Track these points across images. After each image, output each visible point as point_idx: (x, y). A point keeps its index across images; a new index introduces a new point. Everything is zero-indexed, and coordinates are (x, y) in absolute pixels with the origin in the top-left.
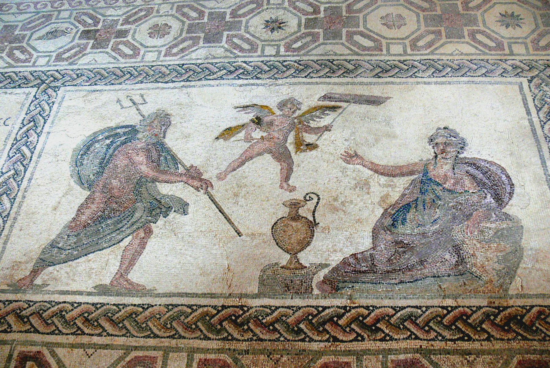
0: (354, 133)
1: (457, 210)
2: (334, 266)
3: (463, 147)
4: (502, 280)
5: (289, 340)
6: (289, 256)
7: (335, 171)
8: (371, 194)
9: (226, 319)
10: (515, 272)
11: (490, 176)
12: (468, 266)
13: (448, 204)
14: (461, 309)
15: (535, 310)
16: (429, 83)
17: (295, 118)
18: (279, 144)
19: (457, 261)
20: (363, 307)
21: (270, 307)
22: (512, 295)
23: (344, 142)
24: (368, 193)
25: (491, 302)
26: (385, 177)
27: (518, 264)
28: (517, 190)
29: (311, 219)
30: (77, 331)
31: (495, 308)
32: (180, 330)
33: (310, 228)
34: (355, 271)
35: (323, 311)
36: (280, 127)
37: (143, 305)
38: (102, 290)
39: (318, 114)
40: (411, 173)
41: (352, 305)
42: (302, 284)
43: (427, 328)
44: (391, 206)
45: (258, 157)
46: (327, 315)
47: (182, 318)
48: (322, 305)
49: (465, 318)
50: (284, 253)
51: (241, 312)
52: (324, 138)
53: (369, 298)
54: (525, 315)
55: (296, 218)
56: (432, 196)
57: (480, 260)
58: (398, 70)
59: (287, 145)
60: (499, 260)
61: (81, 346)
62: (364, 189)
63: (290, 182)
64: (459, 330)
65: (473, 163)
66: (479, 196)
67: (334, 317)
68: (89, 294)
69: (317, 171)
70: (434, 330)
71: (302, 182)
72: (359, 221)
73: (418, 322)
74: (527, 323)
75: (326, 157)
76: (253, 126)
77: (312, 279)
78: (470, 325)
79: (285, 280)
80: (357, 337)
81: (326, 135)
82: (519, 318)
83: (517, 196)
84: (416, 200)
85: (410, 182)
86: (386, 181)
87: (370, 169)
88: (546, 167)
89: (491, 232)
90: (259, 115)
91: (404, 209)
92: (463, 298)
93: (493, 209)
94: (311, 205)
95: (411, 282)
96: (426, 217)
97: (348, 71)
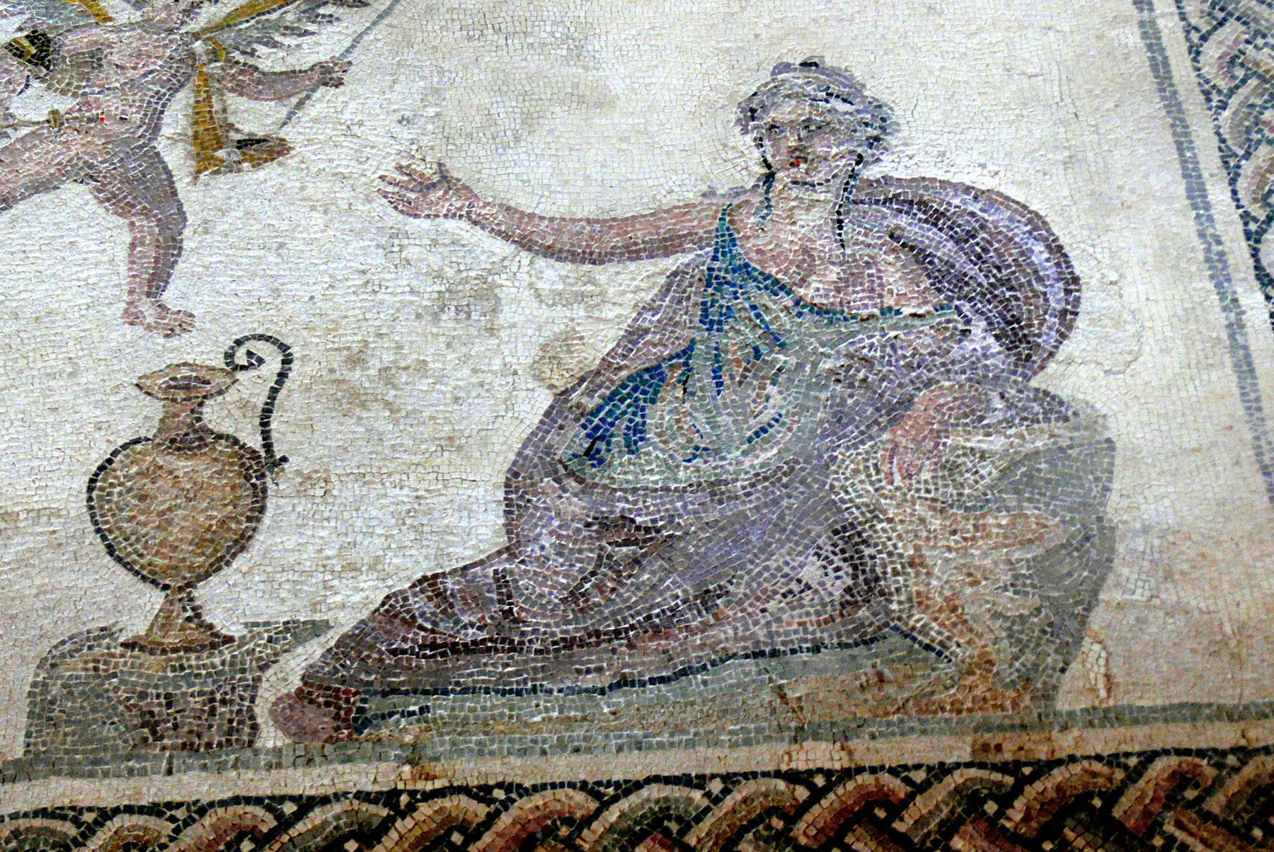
0: (436, 91)
1: (851, 385)
2: (346, 629)
3: (877, 139)
4: (1030, 657)
6: (156, 599)
7: (356, 244)
8: (504, 335)
10: (1083, 623)
11: (985, 250)
12: (894, 606)
13: (815, 365)
14: (866, 779)
15: (1160, 767)
17: (196, 36)
18: (126, 142)
19: (848, 590)
20: (465, 790)
21: (73, 813)
22: (1071, 714)
23: (397, 129)
24: (491, 331)
25: (986, 747)
26: (559, 265)
27: (1095, 593)
28: (1092, 300)
29: (255, 442)
31: (1003, 768)
33: (248, 478)
34: (433, 646)
35: (299, 816)
36: (130, 73)
39: (290, 17)
40: (669, 245)
41: (420, 785)
42: (212, 712)
44: (582, 380)
45: (36, 198)
46: (315, 831)
48: (296, 792)
49: (881, 814)
50: (141, 585)
52: (313, 112)
53: (492, 753)
54: (1120, 791)
55: (190, 439)
56: (752, 337)
57: (941, 577)
59: (161, 145)
60: (1016, 577)
62: (474, 316)
63: (170, 296)
65: (917, 200)
66: (938, 328)
67: (346, 838)
69: (281, 246)
71: (218, 292)
72: (450, 443)
74: (1130, 824)
75: (320, 189)
77: (255, 688)
79: (143, 695)
81: (323, 102)
82: (1097, 802)
83: (1092, 322)
84: (687, 352)
85: (662, 280)
86: (564, 279)
87: (499, 233)
88: (1207, 206)
89: (988, 470)
90: (44, 23)
91: (635, 389)
92: (873, 737)
93: (996, 378)
94: (253, 387)
95: (662, 680)
96: (723, 419)
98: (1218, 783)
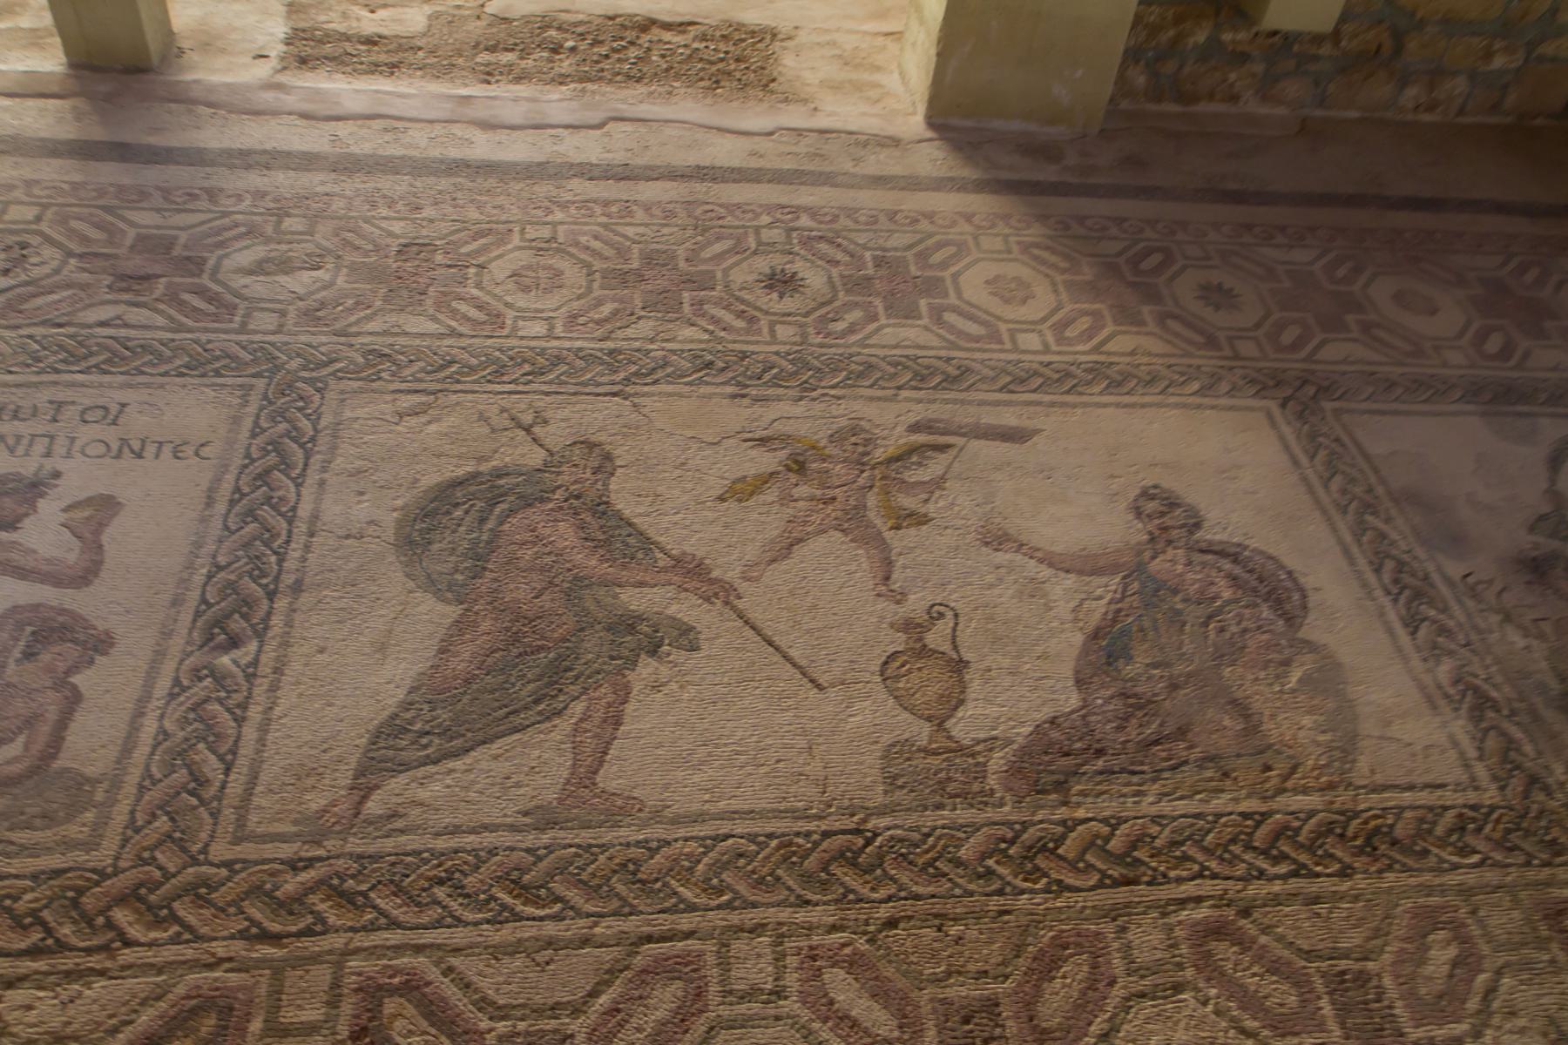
5: (971, 894)
9: (833, 859)
15: (1408, 814)
16: (1105, 405)
30: (500, 914)
32: (742, 888)
35: (1024, 830)
37: (647, 841)
38: (544, 818)
40: (1111, 569)
43: (1226, 856)
47: (742, 862)
51: (860, 842)
55: (923, 652)
58: (1040, 380)
59: (871, 515)
61: (514, 949)
64: (1284, 857)
68: (513, 828)
70: (1243, 861)
73: (1205, 844)
76: (793, 478)
78: (1302, 846)
80: (1100, 880)
97: (950, 381)
98: (1435, 823)
